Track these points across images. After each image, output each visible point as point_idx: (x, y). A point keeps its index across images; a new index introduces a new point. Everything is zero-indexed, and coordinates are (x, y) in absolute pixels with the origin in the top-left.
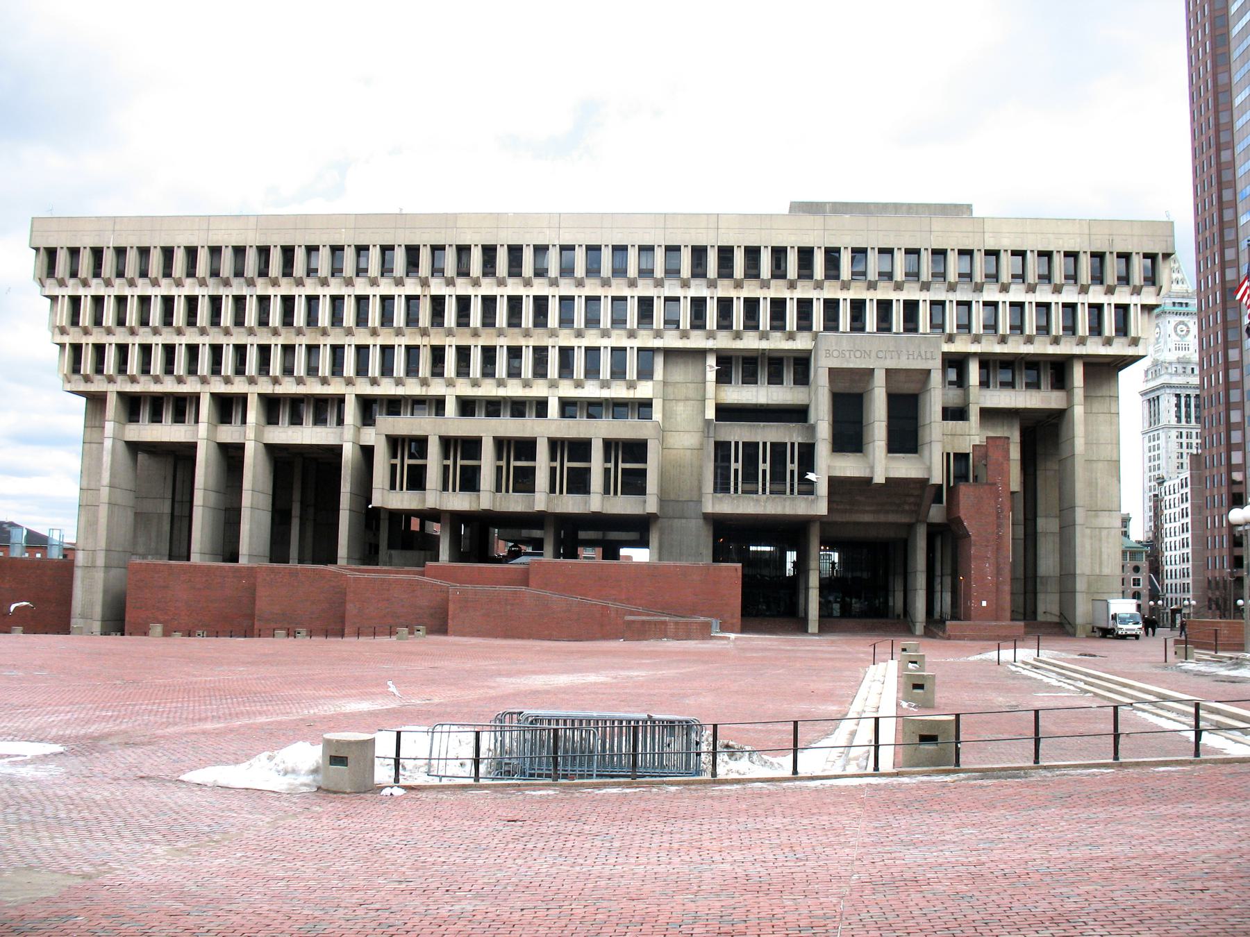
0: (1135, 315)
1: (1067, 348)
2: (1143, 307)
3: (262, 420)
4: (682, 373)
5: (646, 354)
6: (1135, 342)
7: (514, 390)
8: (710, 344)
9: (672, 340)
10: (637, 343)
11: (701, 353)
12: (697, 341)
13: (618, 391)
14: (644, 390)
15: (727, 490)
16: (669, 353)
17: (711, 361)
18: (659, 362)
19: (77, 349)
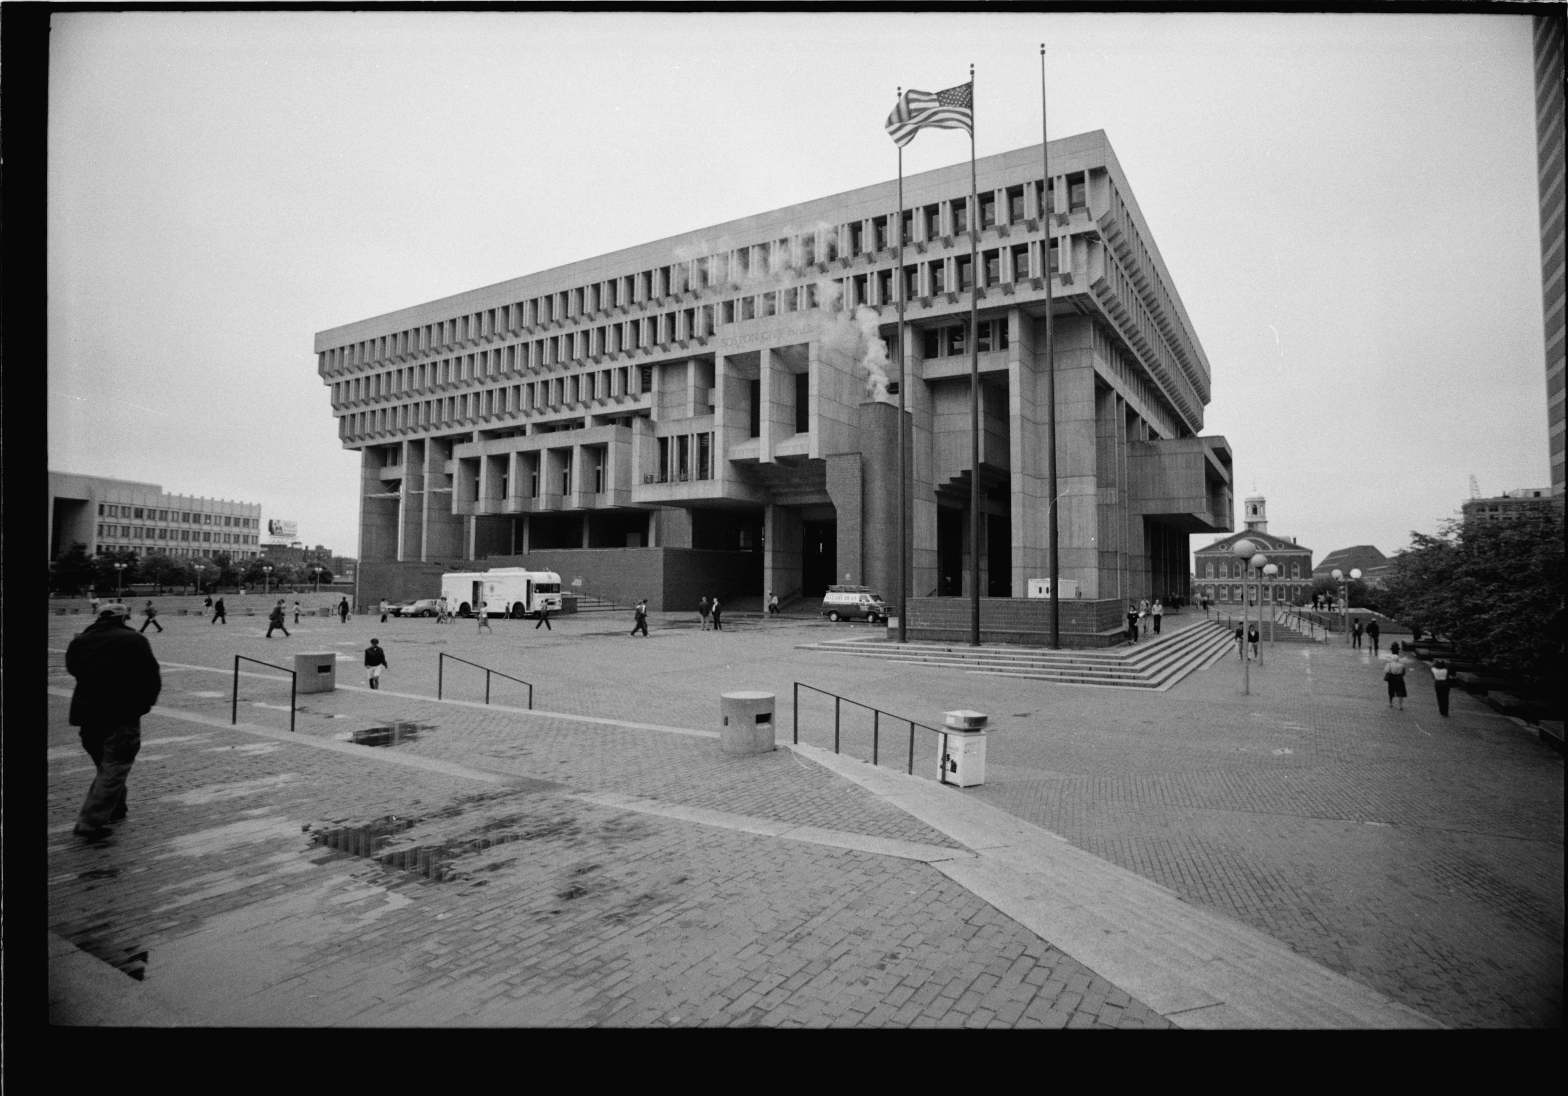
0: (1065, 249)
1: (994, 299)
2: (1076, 238)
3: (438, 457)
4: (673, 384)
5: (645, 370)
6: (1067, 279)
7: (565, 414)
8: (685, 353)
9: (658, 355)
10: (634, 362)
11: (681, 363)
12: (676, 353)
13: (629, 405)
14: (647, 401)
15: (666, 481)
16: (665, 366)
17: (691, 369)
18: (655, 375)
19: (343, 418)
